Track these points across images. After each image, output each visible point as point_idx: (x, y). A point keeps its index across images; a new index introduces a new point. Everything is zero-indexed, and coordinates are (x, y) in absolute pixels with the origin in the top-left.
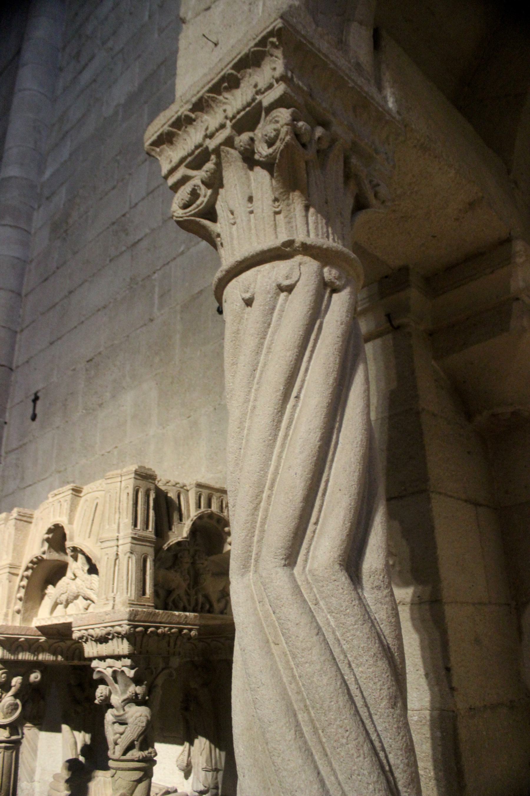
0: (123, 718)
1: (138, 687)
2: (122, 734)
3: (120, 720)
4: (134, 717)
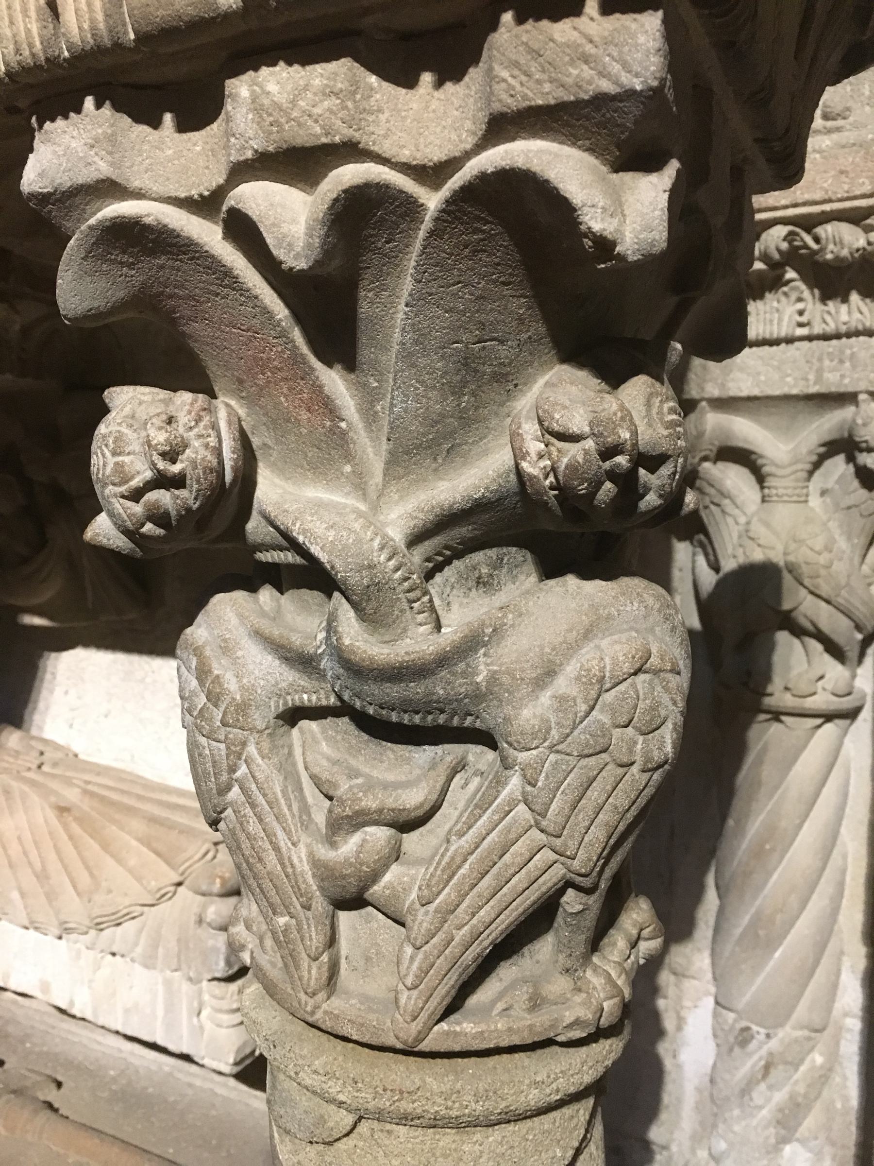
1: (637, 389)
2: (408, 824)
3: (407, 706)
4: (563, 684)
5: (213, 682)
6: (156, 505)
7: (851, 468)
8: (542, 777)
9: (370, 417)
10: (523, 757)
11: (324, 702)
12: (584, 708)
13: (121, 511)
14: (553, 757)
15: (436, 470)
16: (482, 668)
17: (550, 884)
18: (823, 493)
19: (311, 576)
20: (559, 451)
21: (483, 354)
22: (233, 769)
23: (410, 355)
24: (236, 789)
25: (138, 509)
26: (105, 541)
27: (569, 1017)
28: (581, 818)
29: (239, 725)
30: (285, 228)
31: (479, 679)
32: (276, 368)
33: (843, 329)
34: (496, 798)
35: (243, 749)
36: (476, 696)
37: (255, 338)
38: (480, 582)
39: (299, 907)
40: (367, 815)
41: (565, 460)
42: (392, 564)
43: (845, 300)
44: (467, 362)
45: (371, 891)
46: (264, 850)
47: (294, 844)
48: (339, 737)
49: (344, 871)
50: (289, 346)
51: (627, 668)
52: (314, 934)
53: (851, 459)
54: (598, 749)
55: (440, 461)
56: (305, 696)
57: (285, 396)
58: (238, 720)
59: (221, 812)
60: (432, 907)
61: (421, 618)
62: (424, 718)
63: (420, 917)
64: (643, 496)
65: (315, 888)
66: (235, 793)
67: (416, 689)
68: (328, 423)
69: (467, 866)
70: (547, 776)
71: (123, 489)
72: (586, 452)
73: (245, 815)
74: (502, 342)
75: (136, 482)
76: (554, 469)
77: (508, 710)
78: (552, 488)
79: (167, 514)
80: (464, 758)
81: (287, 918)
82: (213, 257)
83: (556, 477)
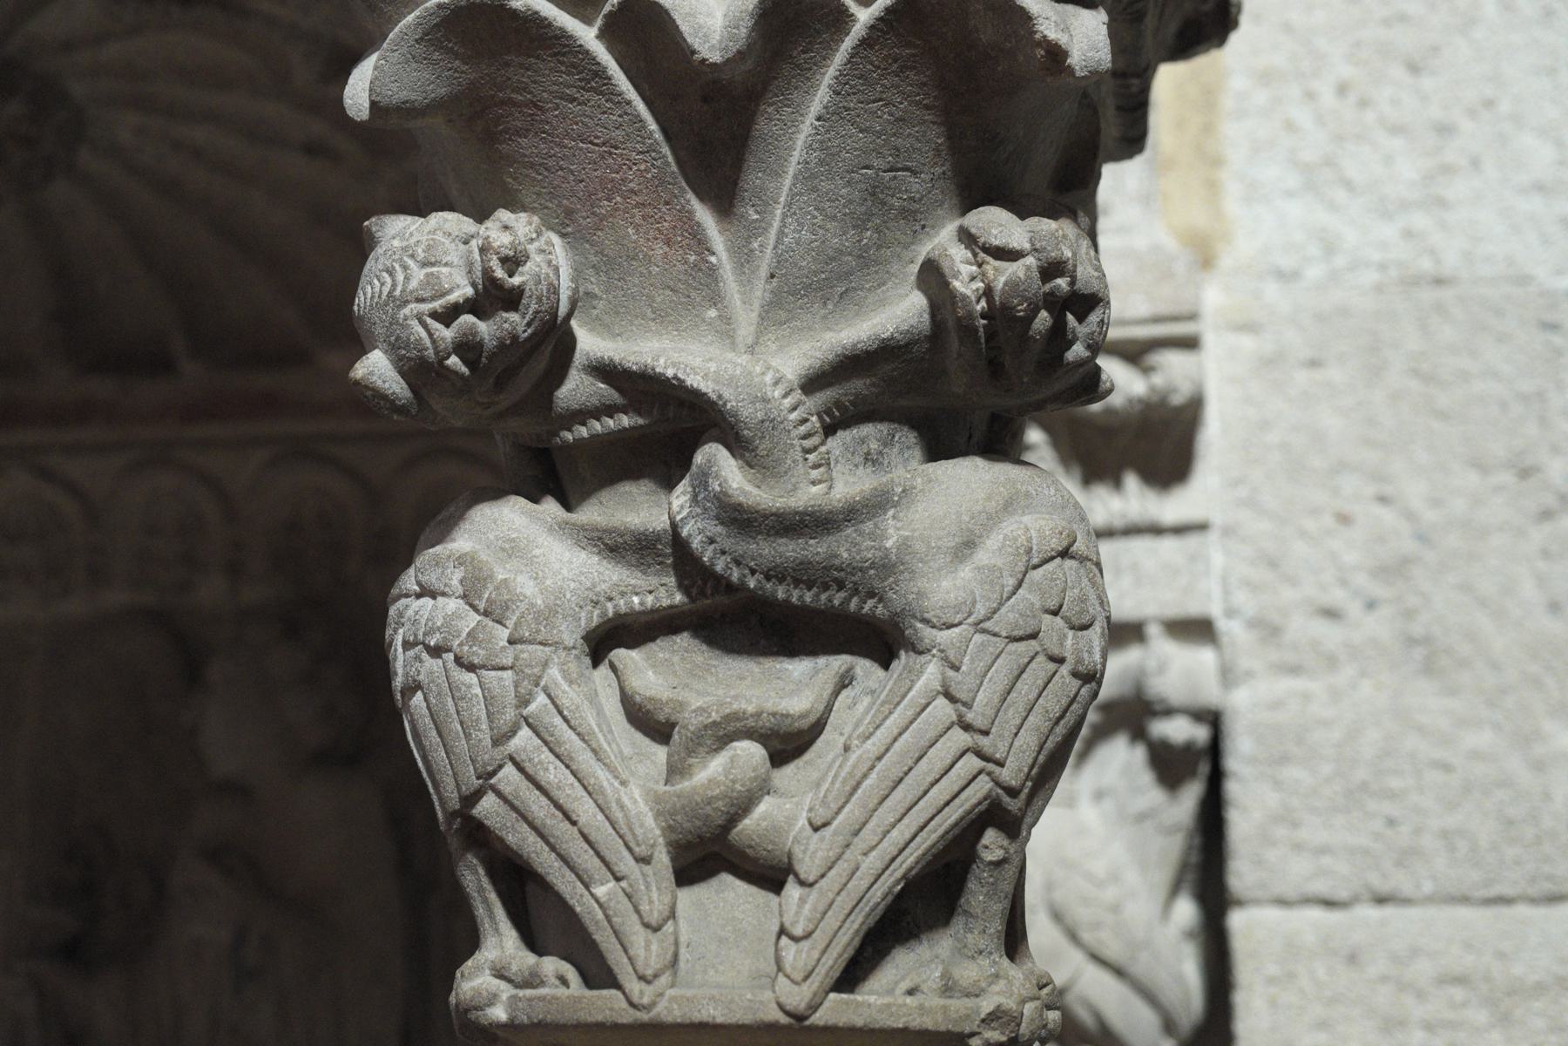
0: (842, 547)
3: (802, 574)
4: (988, 554)
5: (497, 588)
6: (473, 331)
7: (1139, 754)
8: (966, 660)
9: (744, 258)
10: (943, 637)
11: (666, 602)
12: (1011, 582)
13: (424, 334)
14: (978, 638)
15: (824, 317)
16: (893, 531)
17: (974, 801)
18: (1099, 795)
19: (670, 426)
20: (996, 269)
21: (893, 184)
22: (524, 702)
23: (813, 176)
24: (525, 732)
25: (447, 334)
26: (379, 383)
27: (987, 1006)
28: (1012, 715)
29: (540, 638)
30: (701, 20)
31: (889, 544)
32: (632, 191)
33: (1118, 523)
34: (910, 689)
35: (544, 671)
36: (884, 566)
37: (610, 153)
38: (868, 458)
39: (632, 862)
40: (738, 719)
41: (1002, 280)
42: (788, 402)
43: (1117, 483)
44: (874, 192)
45: (740, 827)
46: (576, 799)
47: (623, 783)
48: (676, 659)
49: (710, 793)
50: (658, 163)
51: (1056, 544)
52: (655, 895)
53: (1139, 734)
54: (1029, 631)
55: (830, 307)
56: (636, 600)
57: (637, 227)
58: (538, 631)
59: (494, 773)
60: (827, 832)
61: (815, 474)
62: (817, 595)
63: (812, 847)
64: (1070, 344)
65: (658, 832)
66: (523, 739)
67: (816, 548)
68: (692, 258)
69: (873, 775)
70: (972, 661)
71: (436, 305)
72: (1028, 268)
73: (540, 762)
74: (914, 173)
75: (454, 297)
76: (988, 292)
77: (922, 583)
78: (983, 316)
79: (479, 345)
80: (850, 669)
81: (612, 884)
82: (587, 52)
83: (990, 300)
